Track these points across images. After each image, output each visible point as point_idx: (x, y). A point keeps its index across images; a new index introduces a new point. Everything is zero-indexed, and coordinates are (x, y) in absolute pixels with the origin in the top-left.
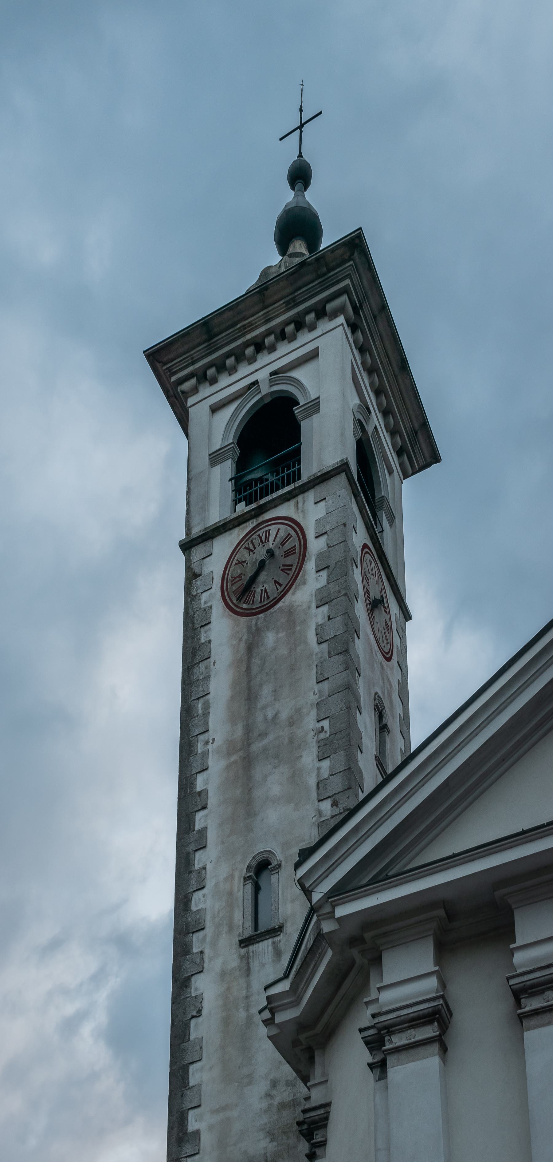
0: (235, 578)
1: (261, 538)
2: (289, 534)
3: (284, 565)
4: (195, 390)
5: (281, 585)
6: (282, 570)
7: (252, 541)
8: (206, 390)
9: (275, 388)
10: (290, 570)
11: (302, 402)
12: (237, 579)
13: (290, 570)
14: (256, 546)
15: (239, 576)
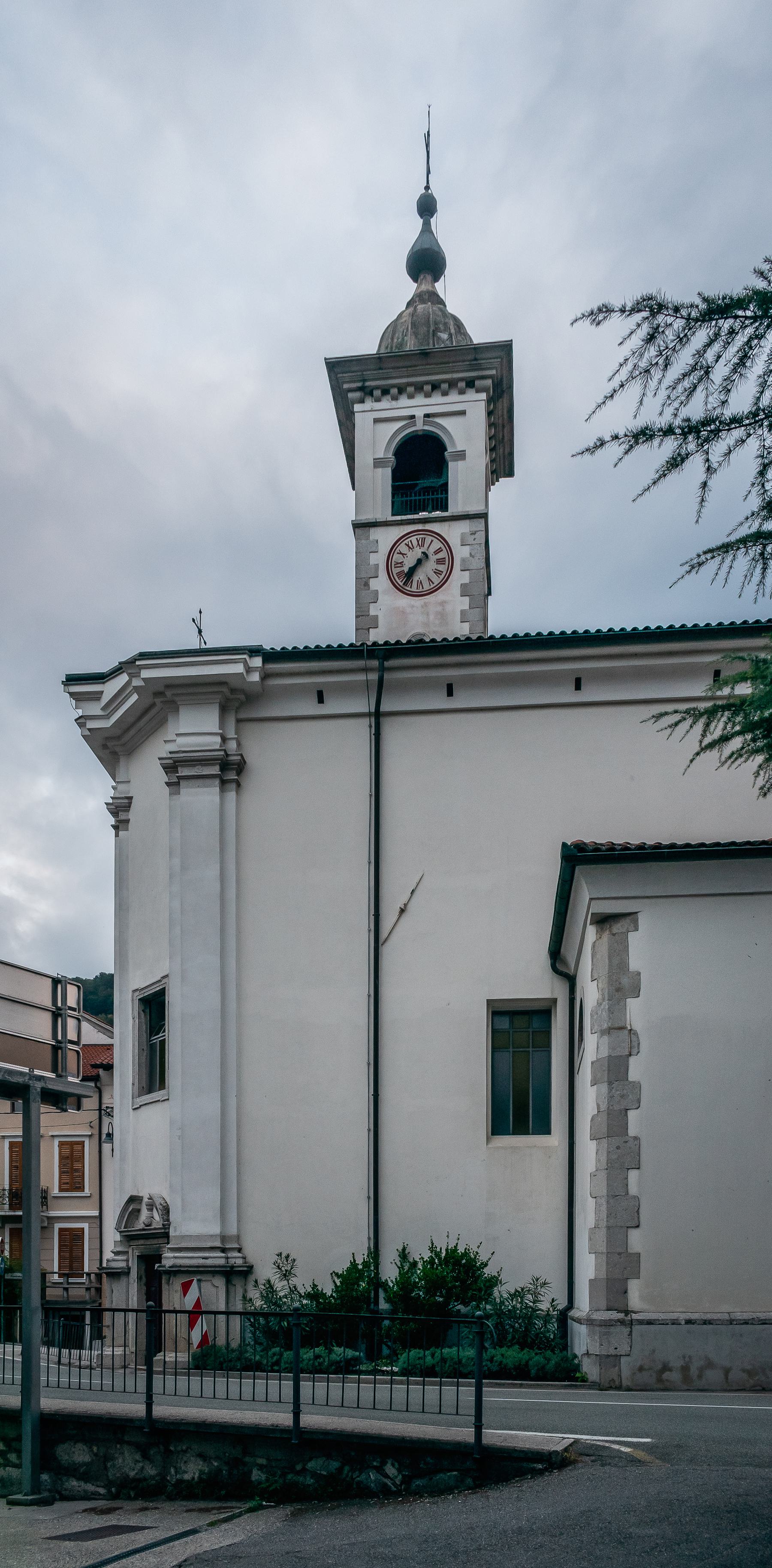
0: (398, 563)
1: (418, 541)
2: (440, 548)
3: (436, 569)
4: (362, 401)
5: (433, 583)
6: (435, 572)
7: (411, 541)
8: (369, 404)
9: (426, 428)
10: (441, 574)
11: (449, 450)
12: (399, 565)
13: (441, 574)
14: (415, 547)
15: (400, 563)
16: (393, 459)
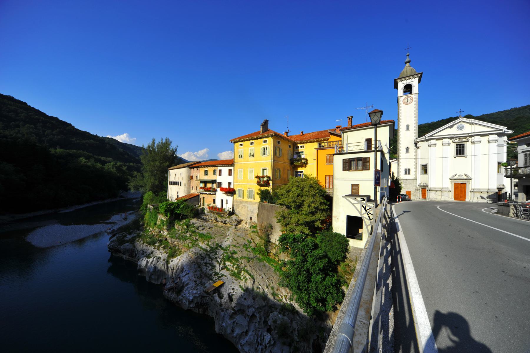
16: (404, 88)
